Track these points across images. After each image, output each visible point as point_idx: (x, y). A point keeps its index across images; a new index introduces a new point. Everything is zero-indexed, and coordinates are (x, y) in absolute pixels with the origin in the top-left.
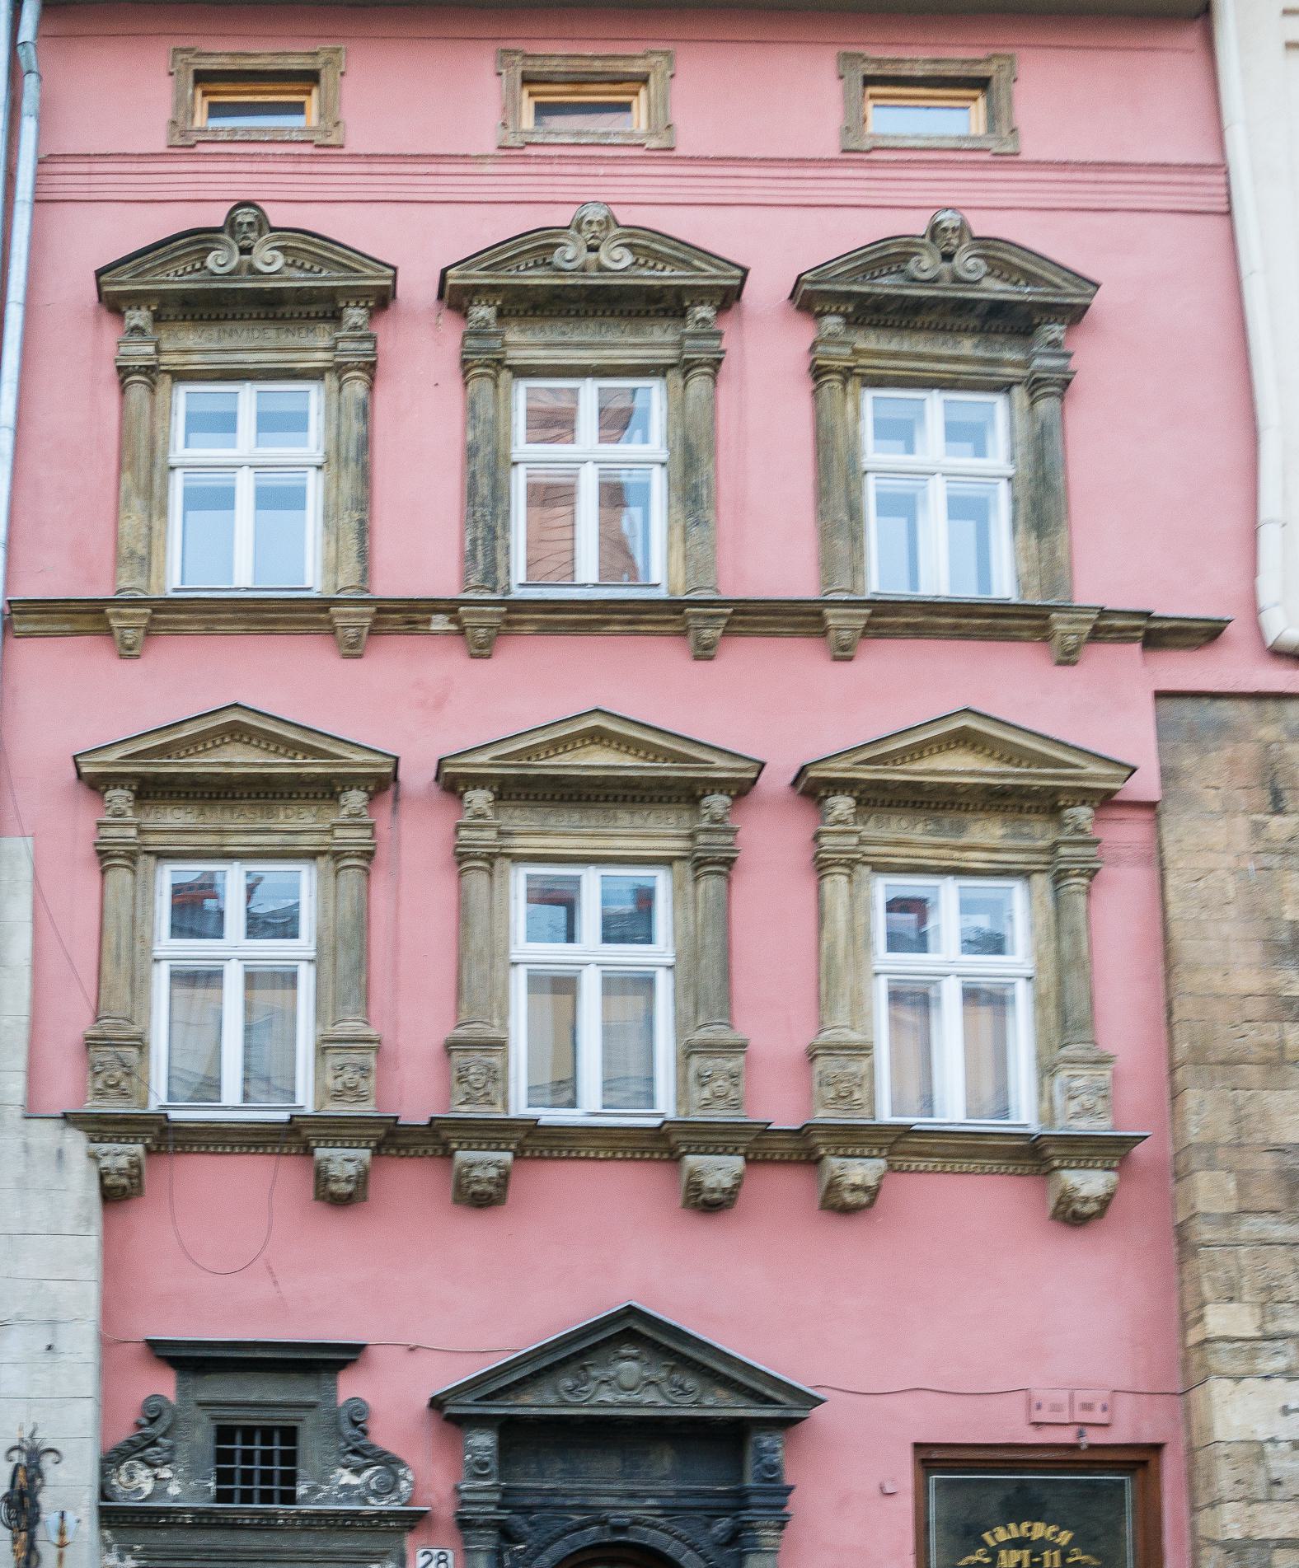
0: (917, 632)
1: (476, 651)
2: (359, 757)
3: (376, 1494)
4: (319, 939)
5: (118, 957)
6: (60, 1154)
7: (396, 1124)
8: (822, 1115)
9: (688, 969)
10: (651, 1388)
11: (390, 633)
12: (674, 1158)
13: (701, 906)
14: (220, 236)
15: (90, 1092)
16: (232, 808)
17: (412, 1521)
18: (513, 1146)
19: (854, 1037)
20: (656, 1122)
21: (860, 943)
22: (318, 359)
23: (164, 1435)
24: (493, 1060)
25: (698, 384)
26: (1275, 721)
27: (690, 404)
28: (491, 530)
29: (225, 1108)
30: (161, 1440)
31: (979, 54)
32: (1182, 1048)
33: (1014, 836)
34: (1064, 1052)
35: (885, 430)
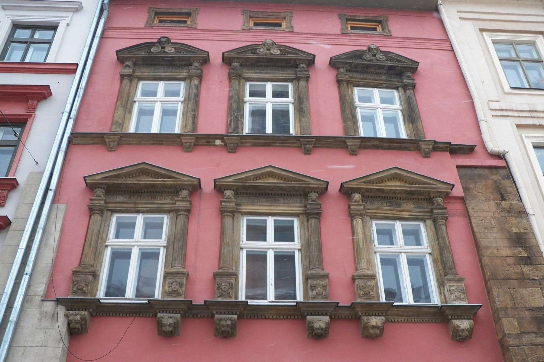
0: (377, 147)
1: (230, 151)
2: (186, 179)
4: (169, 239)
5: (91, 243)
8: (359, 301)
9: (306, 249)
11: (201, 145)
13: (310, 228)
14: (156, 44)
18: (238, 313)
19: (369, 272)
21: (368, 241)
22: (184, 75)
24: (232, 281)
25: (302, 83)
26: (496, 174)
27: (300, 88)
29: (126, 299)
33: (418, 208)
34: (446, 277)
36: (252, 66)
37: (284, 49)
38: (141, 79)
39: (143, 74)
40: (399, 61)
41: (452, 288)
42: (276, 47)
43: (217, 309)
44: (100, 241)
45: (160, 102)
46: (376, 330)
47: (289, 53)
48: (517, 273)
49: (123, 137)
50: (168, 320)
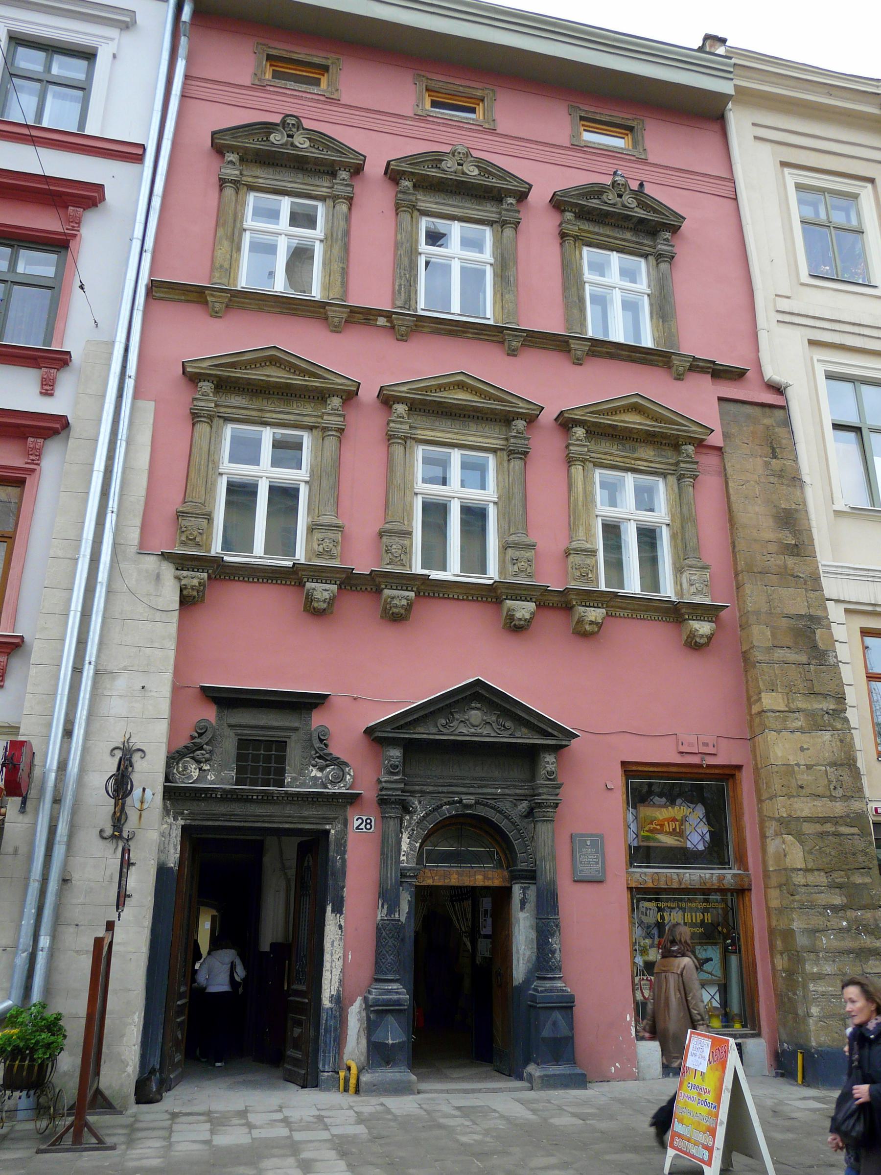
0: (612, 356)
1: (400, 337)
3: (332, 782)
5: (199, 470)
6: (158, 577)
7: (352, 572)
8: (573, 585)
10: (488, 727)
12: (498, 601)
13: (511, 473)
14: (278, 127)
15: (178, 541)
16: (268, 399)
17: (352, 799)
18: (415, 589)
19: (588, 546)
20: (491, 582)
22: (324, 191)
23: (207, 744)
25: (508, 232)
27: (505, 241)
28: (409, 281)
29: (255, 557)
30: (205, 746)
31: (629, 116)
32: (741, 565)
33: (659, 456)
34: (686, 561)
35: (593, 267)
36: (431, 189)
37: (485, 167)
38: (252, 188)
39: (256, 180)
40: (655, 211)
41: (693, 578)
42: (471, 162)
43: (387, 582)
44: (210, 466)
45: (286, 235)
46: (595, 626)
47: (490, 173)
48: (779, 566)
49: (234, 296)
50: (322, 593)
